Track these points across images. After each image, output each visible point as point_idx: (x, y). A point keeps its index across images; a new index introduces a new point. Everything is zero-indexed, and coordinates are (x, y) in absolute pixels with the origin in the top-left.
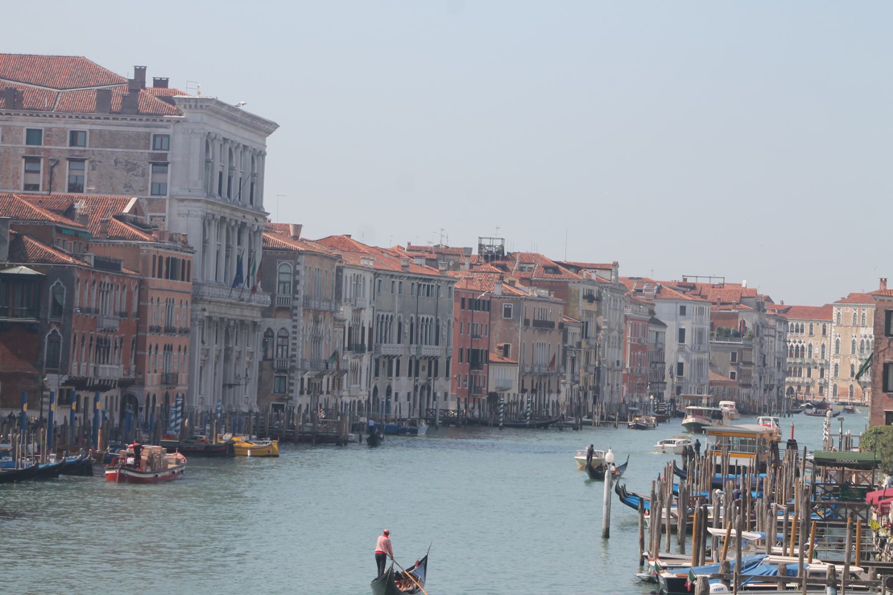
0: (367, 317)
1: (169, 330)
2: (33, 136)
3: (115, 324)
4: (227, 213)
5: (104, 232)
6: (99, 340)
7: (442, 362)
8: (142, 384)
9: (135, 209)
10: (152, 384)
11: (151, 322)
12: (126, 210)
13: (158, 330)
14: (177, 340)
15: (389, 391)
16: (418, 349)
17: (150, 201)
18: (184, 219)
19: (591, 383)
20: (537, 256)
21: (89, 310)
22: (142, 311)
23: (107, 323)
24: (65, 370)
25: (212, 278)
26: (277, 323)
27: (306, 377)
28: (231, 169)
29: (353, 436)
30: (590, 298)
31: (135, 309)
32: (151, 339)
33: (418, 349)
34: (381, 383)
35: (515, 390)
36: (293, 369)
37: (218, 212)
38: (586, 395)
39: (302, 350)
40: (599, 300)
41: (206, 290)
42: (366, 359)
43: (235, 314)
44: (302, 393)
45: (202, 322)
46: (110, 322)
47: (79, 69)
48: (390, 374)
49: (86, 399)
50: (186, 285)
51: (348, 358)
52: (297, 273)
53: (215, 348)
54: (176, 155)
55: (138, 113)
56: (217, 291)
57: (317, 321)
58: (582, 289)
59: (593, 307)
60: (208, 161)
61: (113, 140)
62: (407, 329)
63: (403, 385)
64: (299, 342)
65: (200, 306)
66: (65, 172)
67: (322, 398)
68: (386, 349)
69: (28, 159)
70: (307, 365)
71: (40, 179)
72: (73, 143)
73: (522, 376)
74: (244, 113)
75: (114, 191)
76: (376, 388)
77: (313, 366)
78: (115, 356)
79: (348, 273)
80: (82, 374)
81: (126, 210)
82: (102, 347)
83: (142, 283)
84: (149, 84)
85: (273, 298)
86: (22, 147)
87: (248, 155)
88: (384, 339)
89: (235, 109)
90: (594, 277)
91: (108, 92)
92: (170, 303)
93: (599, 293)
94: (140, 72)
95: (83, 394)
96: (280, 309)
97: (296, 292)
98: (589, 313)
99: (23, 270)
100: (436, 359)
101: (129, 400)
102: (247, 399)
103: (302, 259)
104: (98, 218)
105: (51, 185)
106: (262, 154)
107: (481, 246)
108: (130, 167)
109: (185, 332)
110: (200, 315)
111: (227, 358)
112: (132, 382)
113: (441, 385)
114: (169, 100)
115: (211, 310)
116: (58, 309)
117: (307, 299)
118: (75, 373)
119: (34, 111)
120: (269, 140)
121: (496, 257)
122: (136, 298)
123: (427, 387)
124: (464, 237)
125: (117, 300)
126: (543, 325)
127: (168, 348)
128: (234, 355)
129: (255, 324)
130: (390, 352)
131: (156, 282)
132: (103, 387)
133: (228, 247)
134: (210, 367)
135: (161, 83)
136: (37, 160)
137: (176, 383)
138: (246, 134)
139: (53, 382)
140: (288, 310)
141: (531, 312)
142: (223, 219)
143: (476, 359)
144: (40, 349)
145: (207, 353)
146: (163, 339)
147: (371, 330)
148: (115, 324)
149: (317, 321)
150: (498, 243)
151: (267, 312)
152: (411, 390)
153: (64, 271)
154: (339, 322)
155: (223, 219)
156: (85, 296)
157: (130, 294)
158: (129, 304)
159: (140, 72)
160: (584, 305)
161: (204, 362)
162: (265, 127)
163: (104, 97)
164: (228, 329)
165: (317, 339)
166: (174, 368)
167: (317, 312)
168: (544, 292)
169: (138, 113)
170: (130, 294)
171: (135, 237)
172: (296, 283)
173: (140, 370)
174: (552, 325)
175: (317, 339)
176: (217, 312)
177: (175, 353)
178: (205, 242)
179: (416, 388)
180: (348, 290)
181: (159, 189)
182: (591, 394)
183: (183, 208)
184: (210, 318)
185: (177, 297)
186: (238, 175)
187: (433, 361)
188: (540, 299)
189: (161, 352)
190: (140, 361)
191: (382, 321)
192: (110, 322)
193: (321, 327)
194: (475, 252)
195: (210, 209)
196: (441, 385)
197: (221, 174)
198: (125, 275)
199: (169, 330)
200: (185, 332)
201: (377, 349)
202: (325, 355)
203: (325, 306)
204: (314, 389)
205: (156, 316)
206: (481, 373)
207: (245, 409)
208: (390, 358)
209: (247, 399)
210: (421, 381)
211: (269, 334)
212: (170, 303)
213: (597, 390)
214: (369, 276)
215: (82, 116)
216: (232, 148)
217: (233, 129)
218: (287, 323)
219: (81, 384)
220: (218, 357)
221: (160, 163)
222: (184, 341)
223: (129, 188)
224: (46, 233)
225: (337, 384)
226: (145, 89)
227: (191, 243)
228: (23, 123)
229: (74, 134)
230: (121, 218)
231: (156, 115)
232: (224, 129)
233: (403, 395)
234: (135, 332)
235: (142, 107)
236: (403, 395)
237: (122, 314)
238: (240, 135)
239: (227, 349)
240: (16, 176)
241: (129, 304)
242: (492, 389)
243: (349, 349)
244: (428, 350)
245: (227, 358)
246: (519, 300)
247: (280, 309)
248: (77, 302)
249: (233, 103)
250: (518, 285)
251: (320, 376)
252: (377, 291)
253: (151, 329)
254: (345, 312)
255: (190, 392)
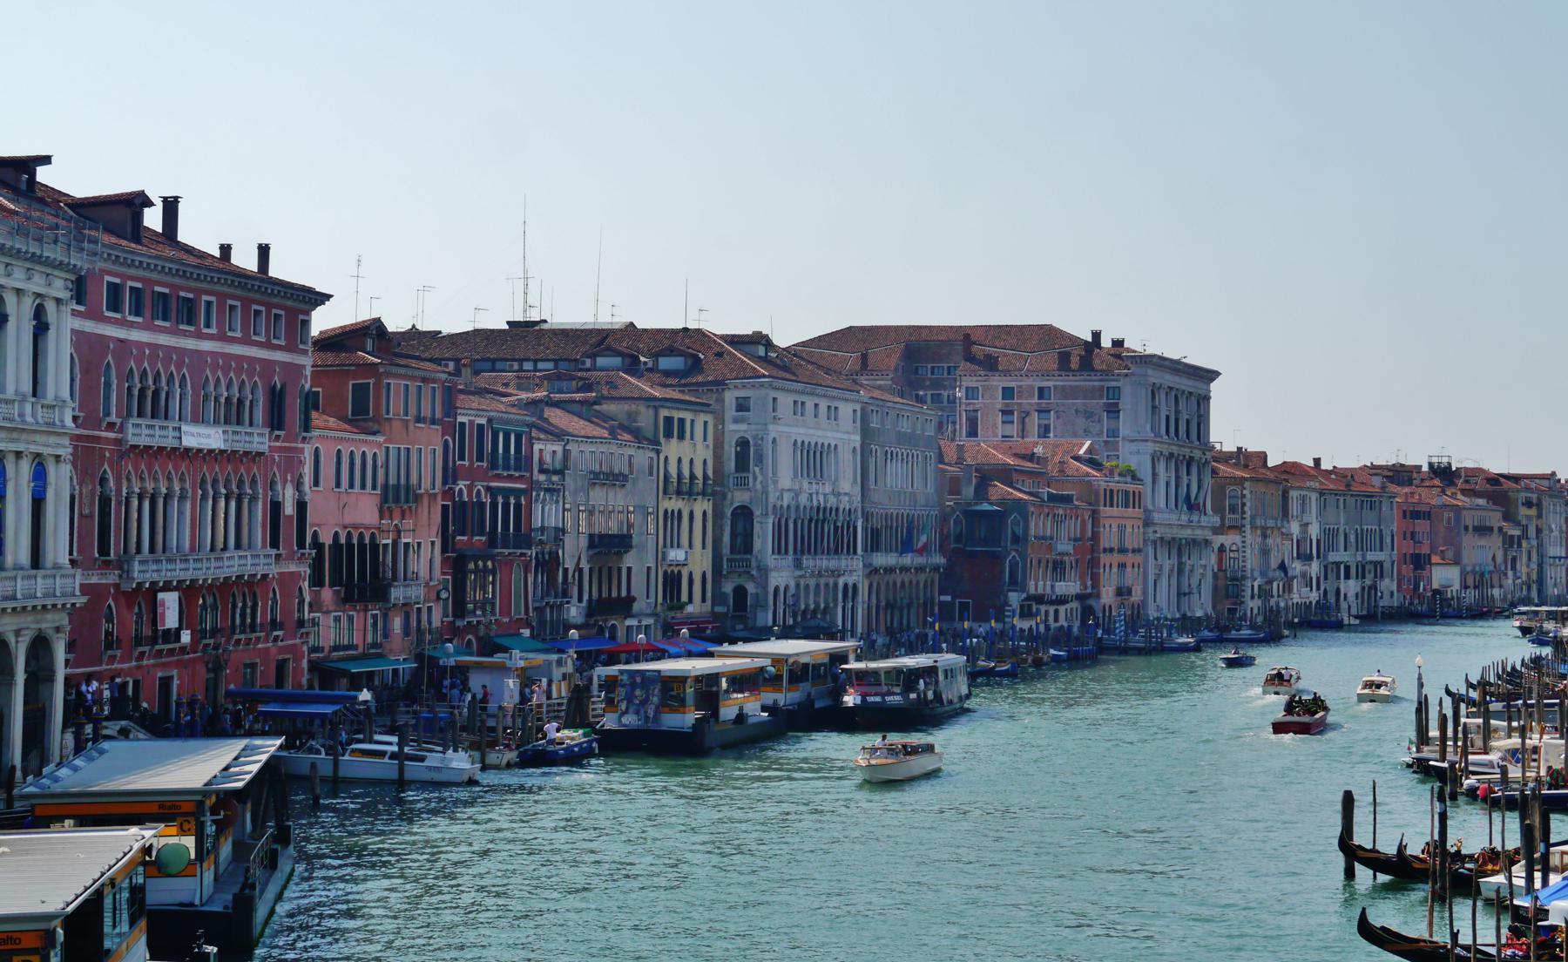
0: (1314, 531)
1: (1122, 550)
2: (1008, 393)
3: (1069, 548)
4: (1175, 449)
5: (1062, 471)
6: (1055, 563)
7: (1387, 566)
8: (1098, 596)
9: (1089, 451)
10: (1107, 596)
11: (1105, 542)
12: (1082, 452)
13: (1111, 550)
14: (1130, 558)
15: (1338, 591)
16: (1364, 556)
17: (1106, 442)
18: (1134, 455)
19: (1534, 577)
20: (1480, 470)
21: (1044, 538)
22: (1095, 536)
23: (1061, 548)
24: (1023, 589)
25: (1163, 504)
26: (1228, 539)
27: (1256, 584)
28: (1177, 412)
29: (1286, 632)
30: (1529, 504)
31: (1089, 534)
32: (1105, 559)
33: (1364, 556)
34: (1329, 586)
35: (1457, 586)
36: (1244, 578)
37: (1166, 450)
38: (1529, 588)
39: (1251, 562)
40: (1539, 505)
41: (1157, 517)
42: (1315, 568)
43: (1186, 533)
44: (1252, 597)
45: (1155, 543)
46: (1065, 546)
47: (1047, 335)
48: (1338, 578)
49: (1047, 612)
50: (1137, 512)
51: (1297, 567)
52: (1243, 496)
53: (1168, 563)
54: (1125, 403)
55: (1093, 370)
56: (1165, 516)
57: (1265, 536)
58: (1522, 496)
59: (1533, 512)
60: (1154, 407)
61: (1071, 393)
62: (1352, 538)
63: (1351, 587)
64: (1248, 554)
65: (1151, 530)
66: (1034, 421)
67: (1272, 602)
68: (1333, 557)
69: (1004, 412)
70: (1257, 574)
71: (1014, 429)
72: (1041, 397)
73: (1464, 575)
74: (1186, 365)
75: (1075, 435)
76: (1325, 591)
77: (1263, 574)
78: (1072, 574)
79: (1294, 494)
80: (1040, 591)
81: (1082, 452)
82: (1058, 568)
83: (1095, 513)
84: (1106, 343)
85: (1223, 519)
86: (999, 402)
87: (1194, 401)
88: (1332, 547)
89: (1178, 362)
90: (1533, 485)
91: (1068, 354)
92: (1122, 529)
93: (1539, 499)
94: (1097, 335)
95: (1043, 608)
96: (1230, 527)
97: (1243, 512)
98: (1528, 517)
99: (986, 507)
100: (1381, 563)
101: (1088, 611)
102: (1201, 606)
103: (1247, 484)
104: (1057, 459)
105: (1023, 433)
106: (1207, 398)
107: (1431, 465)
108: (1088, 415)
109: (1136, 551)
110: (1152, 536)
111: (1180, 572)
112: (1089, 596)
113: (1388, 585)
114: (1118, 356)
115: (1161, 531)
116: (1016, 539)
117: (1253, 517)
118: (1032, 591)
119: (1007, 373)
120: (1213, 386)
121: (1444, 474)
122: (1089, 526)
123: (1374, 587)
124: (1418, 457)
125: (1072, 527)
126: (1483, 530)
127: (1122, 566)
128: (1187, 568)
129: (1206, 541)
130: (1338, 559)
131: (1105, 511)
132: (1062, 600)
133: (1177, 478)
134: (1164, 581)
135: (1118, 343)
136: (1011, 413)
137: (1129, 593)
138: (1191, 383)
139: (1015, 598)
140: (1238, 528)
141: (1469, 519)
142: (1171, 455)
143: (1420, 562)
144: (1003, 572)
145: (1161, 568)
146: (1116, 558)
147: (1318, 541)
148: (1069, 548)
149: (1265, 536)
150: (1445, 460)
151: (1217, 531)
152: (1359, 589)
153: (1019, 505)
154: (1289, 536)
155: (1171, 455)
156: (1038, 526)
157: (1083, 522)
158: (1083, 530)
159: (1097, 335)
160: (1523, 511)
161: (1158, 576)
162: (1212, 375)
163: (1064, 359)
164: (1180, 548)
165: (1265, 552)
166: (1128, 582)
167: (1264, 529)
168: (1482, 502)
169: (1093, 370)
170: (1083, 522)
171: (1088, 474)
172: (1244, 505)
173: (1096, 585)
174: (1491, 529)
175: (1265, 552)
176: (1169, 534)
177: (1129, 569)
178: (1155, 475)
179: (1363, 588)
180: (1294, 508)
181: (1114, 433)
182: (1534, 587)
183: (1134, 447)
184: (1162, 539)
185: (1129, 524)
186: (1184, 417)
187: (1378, 565)
188: (1479, 508)
189: (1115, 570)
190: (1095, 578)
191: (1329, 535)
192: (1065, 546)
193: (1270, 541)
194: (1425, 468)
195: (1157, 447)
196: (1388, 585)
197: (1168, 418)
198: (1077, 507)
199: (1122, 550)
200: (1139, 551)
201: (1325, 557)
202: (1274, 564)
203: (1271, 523)
204: (1264, 594)
205: (1109, 538)
206: (1425, 573)
207: (1199, 614)
208: (1338, 564)
209: (1201, 606)
210: (1368, 582)
211: (1222, 549)
212: (1122, 529)
213: (1541, 581)
214: (1314, 496)
215: (1047, 375)
216: (1177, 395)
217: (1177, 379)
218: (1237, 538)
219: (1040, 599)
220: (1171, 571)
221: (1113, 411)
222: (1138, 558)
223: (1087, 433)
224: (1006, 475)
225: (1288, 588)
226: (1100, 347)
227: (1139, 475)
228: (998, 382)
229: (1041, 390)
230: (1077, 458)
231: (1107, 372)
232: (1169, 379)
233: (1351, 595)
234: (1090, 556)
235: (1097, 363)
236: (1351, 595)
237: (1075, 540)
238: (1184, 384)
239: (1181, 565)
240: (995, 426)
241: (1083, 530)
242: (1435, 586)
243: (1298, 557)
244: (1371, 556)
245: (1180, 572)
246: (1457, 510)
247: (1230, 527)
248: (1032, 532)
249: (1175, 357)
250: (1459, 496)
251: (1270, 582)
252: (1323, 508)
253: (1105, 550)
254: (1295, 528)
255: (1143, 604)
